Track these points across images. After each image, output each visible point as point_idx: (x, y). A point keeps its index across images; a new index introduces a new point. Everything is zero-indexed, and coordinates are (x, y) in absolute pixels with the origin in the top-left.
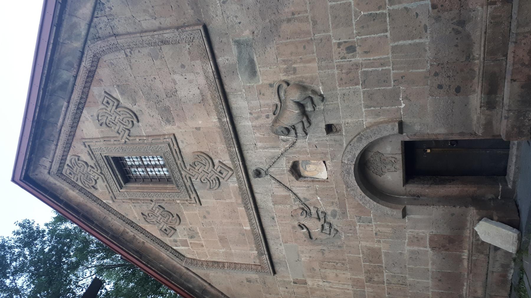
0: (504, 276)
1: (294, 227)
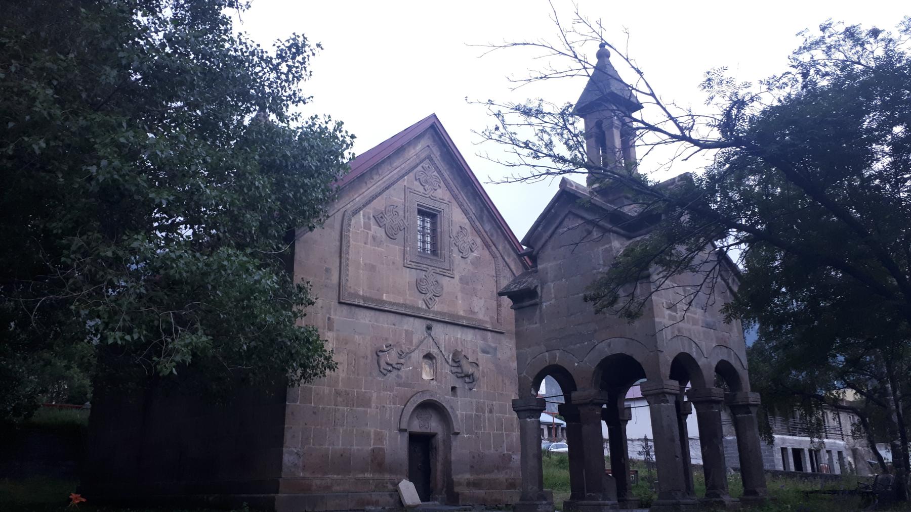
0: (368, 504)
1: (387, 339)
